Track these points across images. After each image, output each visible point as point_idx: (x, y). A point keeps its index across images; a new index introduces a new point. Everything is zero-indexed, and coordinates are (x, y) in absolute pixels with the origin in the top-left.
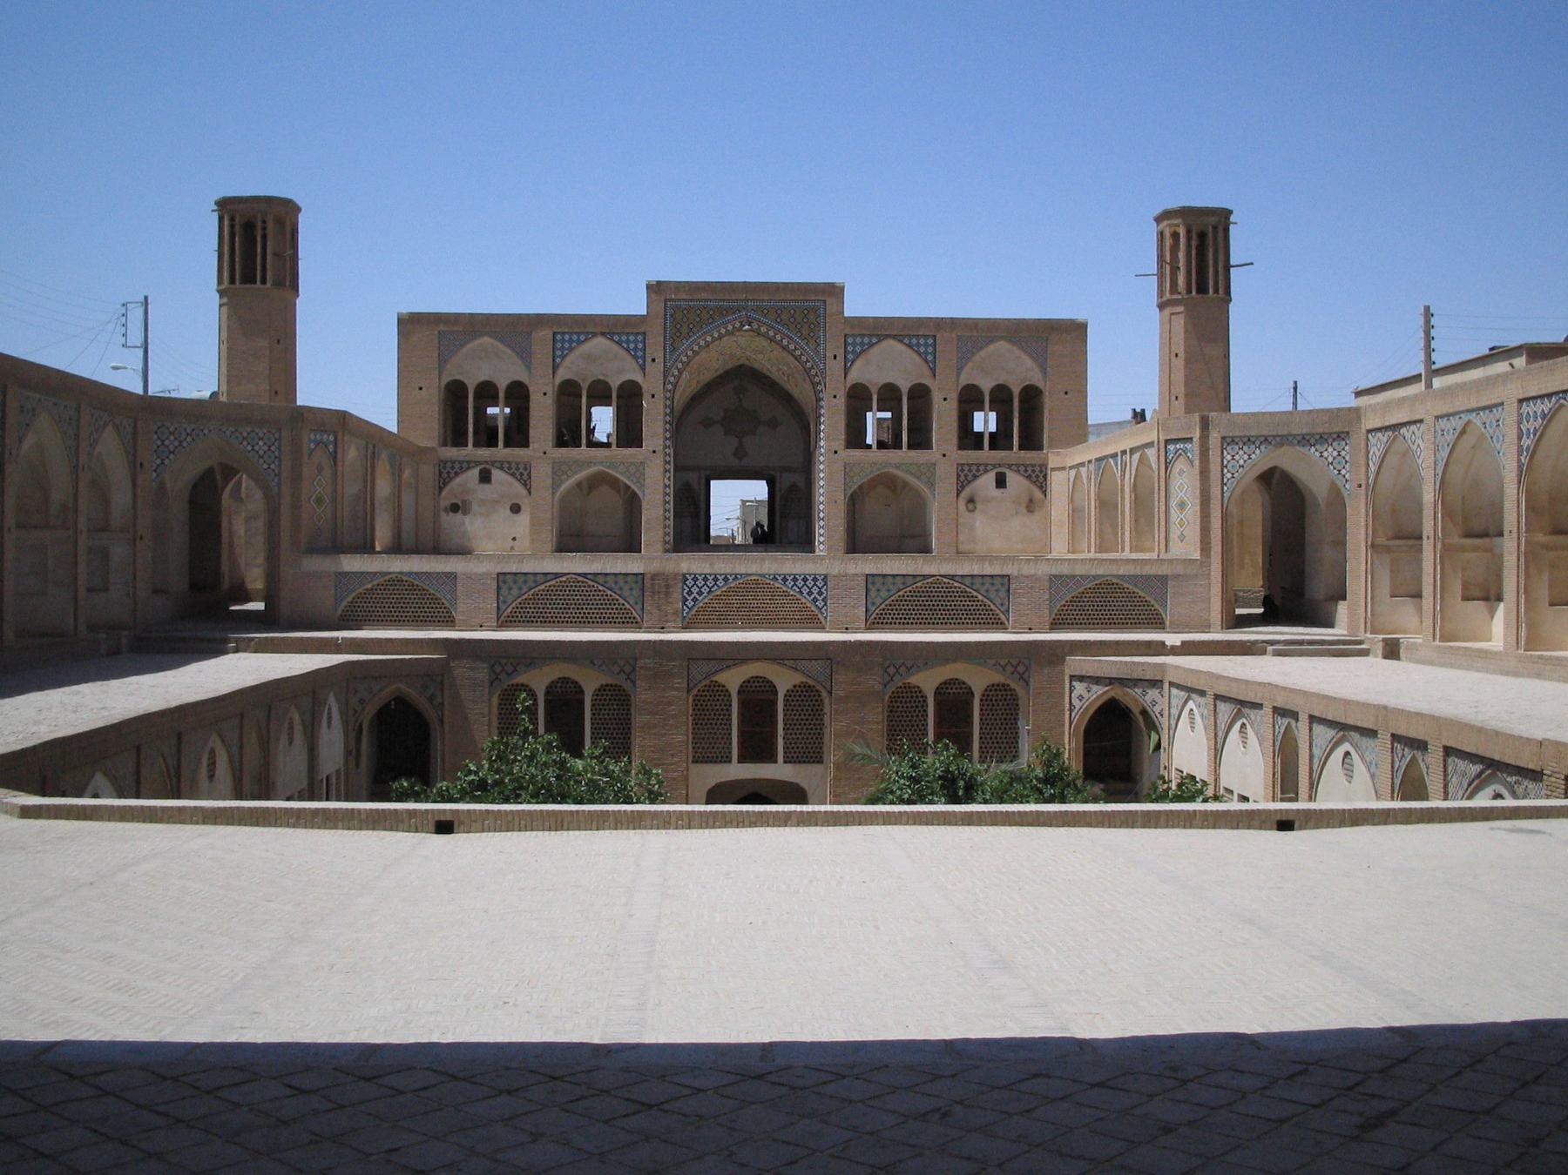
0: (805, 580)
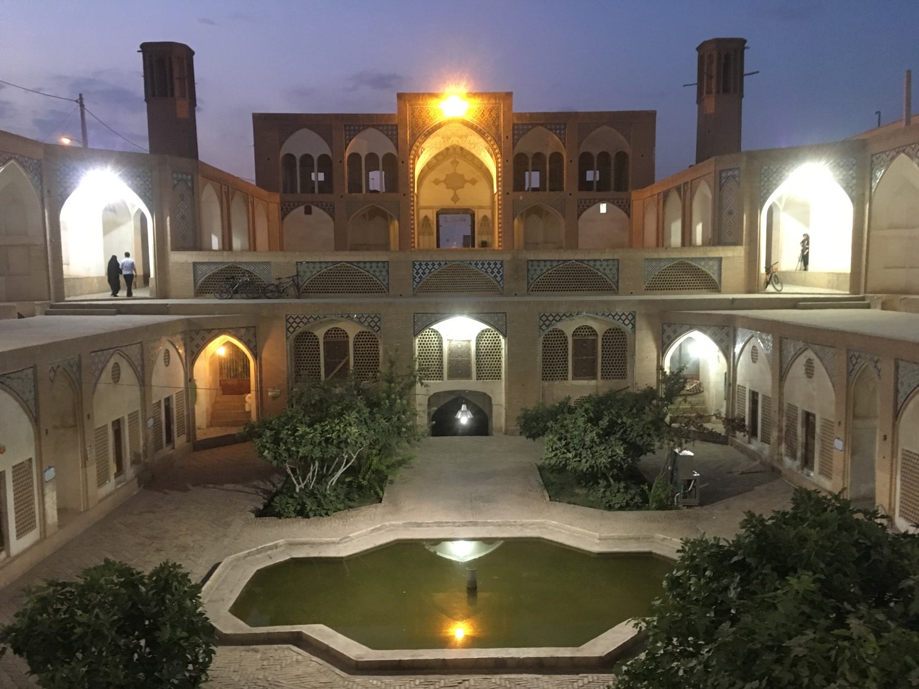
0: (489, 264)
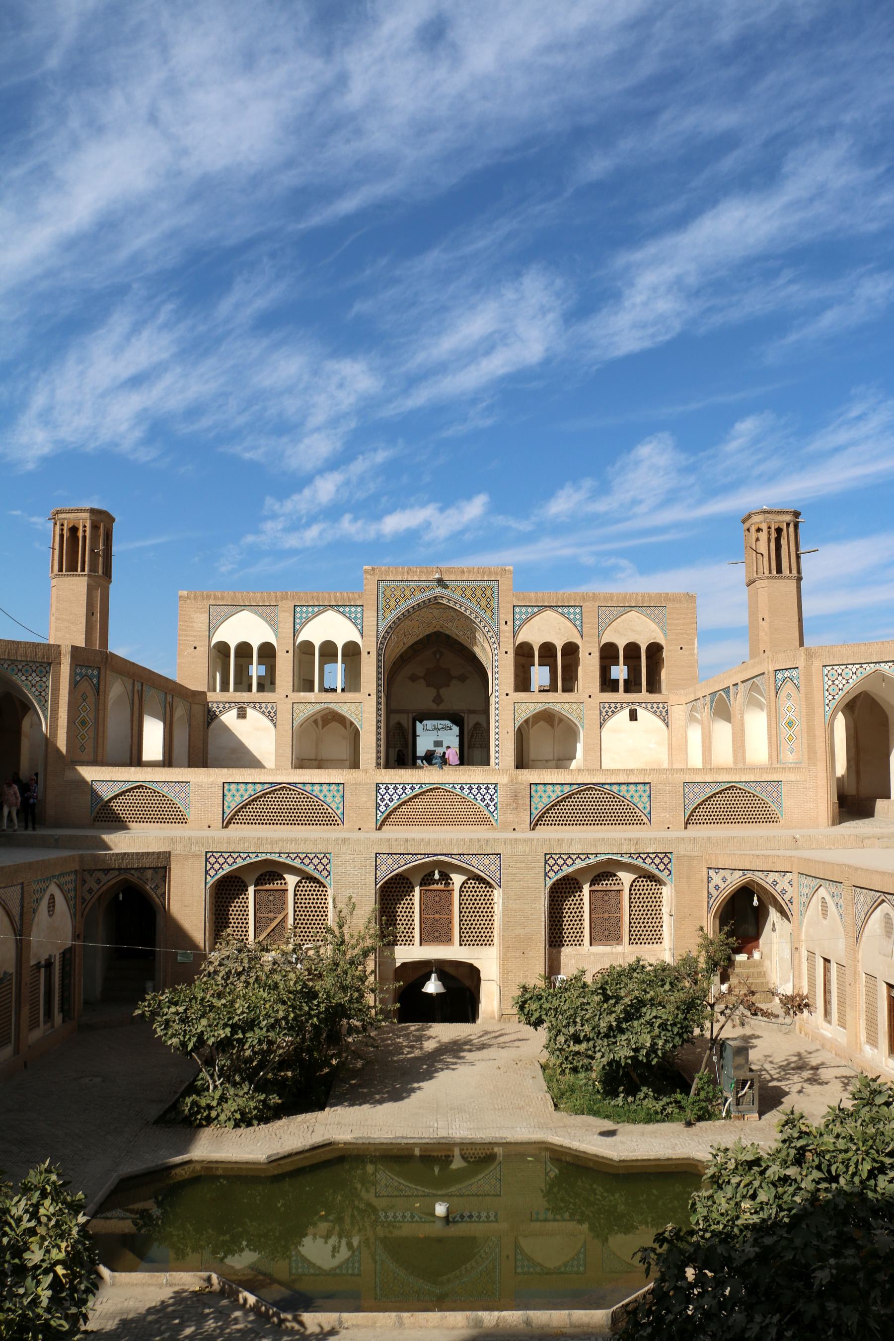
0: (479, 788)
